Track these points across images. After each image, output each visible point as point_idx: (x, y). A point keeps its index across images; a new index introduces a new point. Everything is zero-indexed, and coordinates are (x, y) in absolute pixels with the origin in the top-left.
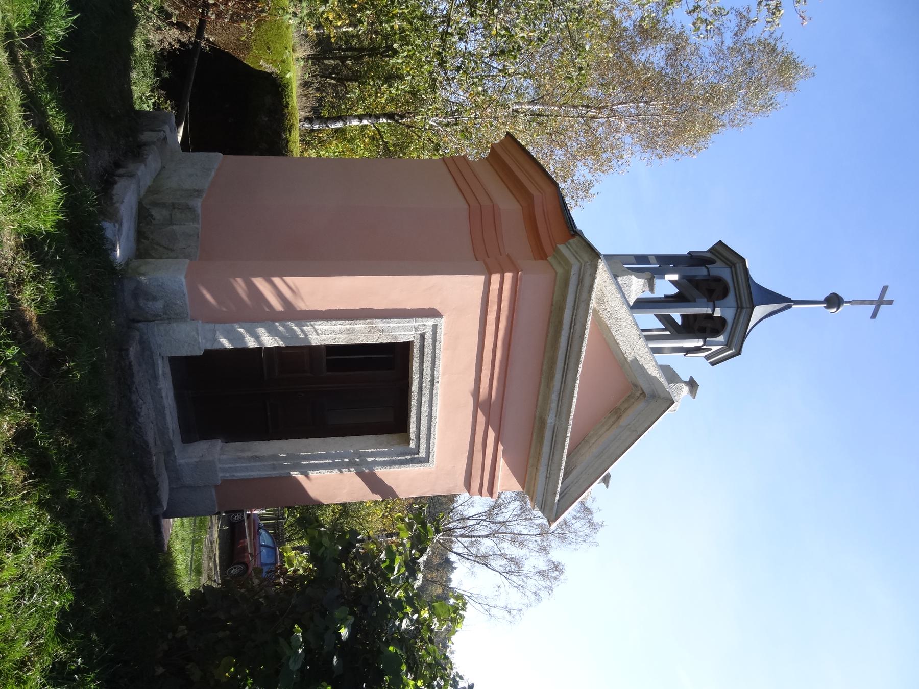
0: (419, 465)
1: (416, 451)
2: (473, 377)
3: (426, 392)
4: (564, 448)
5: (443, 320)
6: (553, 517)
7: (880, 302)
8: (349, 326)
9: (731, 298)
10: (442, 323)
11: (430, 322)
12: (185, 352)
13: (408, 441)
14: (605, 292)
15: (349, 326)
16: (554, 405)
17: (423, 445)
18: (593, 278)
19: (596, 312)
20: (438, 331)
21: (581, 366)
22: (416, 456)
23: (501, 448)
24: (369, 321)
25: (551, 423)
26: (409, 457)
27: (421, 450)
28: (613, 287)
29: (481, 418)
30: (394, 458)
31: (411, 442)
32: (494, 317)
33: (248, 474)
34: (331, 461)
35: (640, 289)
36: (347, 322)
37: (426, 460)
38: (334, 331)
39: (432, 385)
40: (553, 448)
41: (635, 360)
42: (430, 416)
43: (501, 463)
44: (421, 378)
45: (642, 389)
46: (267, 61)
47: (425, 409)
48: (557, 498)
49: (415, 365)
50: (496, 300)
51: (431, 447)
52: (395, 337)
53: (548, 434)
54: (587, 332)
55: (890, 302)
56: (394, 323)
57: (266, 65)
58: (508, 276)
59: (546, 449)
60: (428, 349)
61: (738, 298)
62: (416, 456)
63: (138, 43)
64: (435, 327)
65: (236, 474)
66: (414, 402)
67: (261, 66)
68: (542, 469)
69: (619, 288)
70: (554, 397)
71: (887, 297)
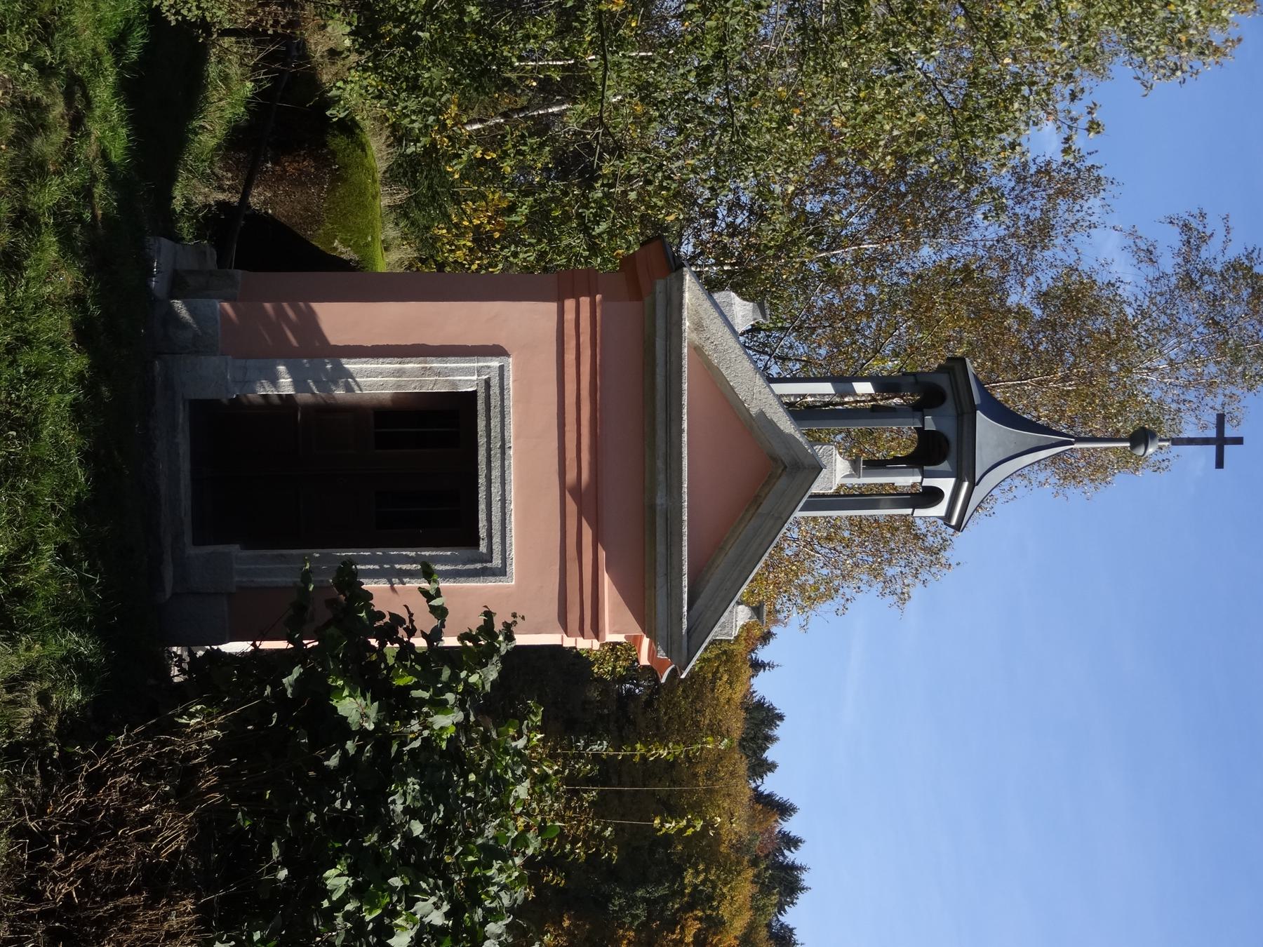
1: (488, 558)
2: (555, 444)
3: (496, 464)
5: (511, 360)
6: (684, 659)
7: (1221, 442)
8: (398, 366)
9: (949, 407)
10: (510, 362)
11: (495, 363)
12: (209, 394)
13: (476, 544)
14: (702, 314)
15: (398, 366)
16: (661, 477)
17: (497, 547)
19: (697, 349)
20: (506, 374)
21: (685, 411)
22: (489, 565)
23: (602, 555)
24: (421, 359)
25: (662, 505)
26: (479, 566)
27: (495, 556)
28: (707, 304)
29: (572, 507)
30: (460, 567)
31: (481, 542)
32: (574, 357)
33: (269, 580)
34: (377, 567)
35: (750, 316)
36: (396, 360)
37: (502, 572)
38: (381, 373)
39: (503, 453)
40: (669, 546)
41: (762, 414)
42: (503, 500)
43: (606, 581)
44: (489, 442)
45: (783, 463)
46: (343, 242)
47: (496, 489)
48: (685, 626)
49: (481, 424)
50: (573, 333)
51: (508, 549)
52: (453, 383)
53: (660, 522)
54: (685, 362)
55: (1238, 441)
57: (341, 248)
58: (585, 301)
59: (661, 549)
60: (495, 401)
61: (958, 404)
62: (489, 565)
63: (178, 204)
64: (501, 368)
65: (255, 579)
66: (482, 480)
67: (336, 249)
68: (660, 581)
69: (715, 305)
70: (660, 464)
71: (1229, 432)
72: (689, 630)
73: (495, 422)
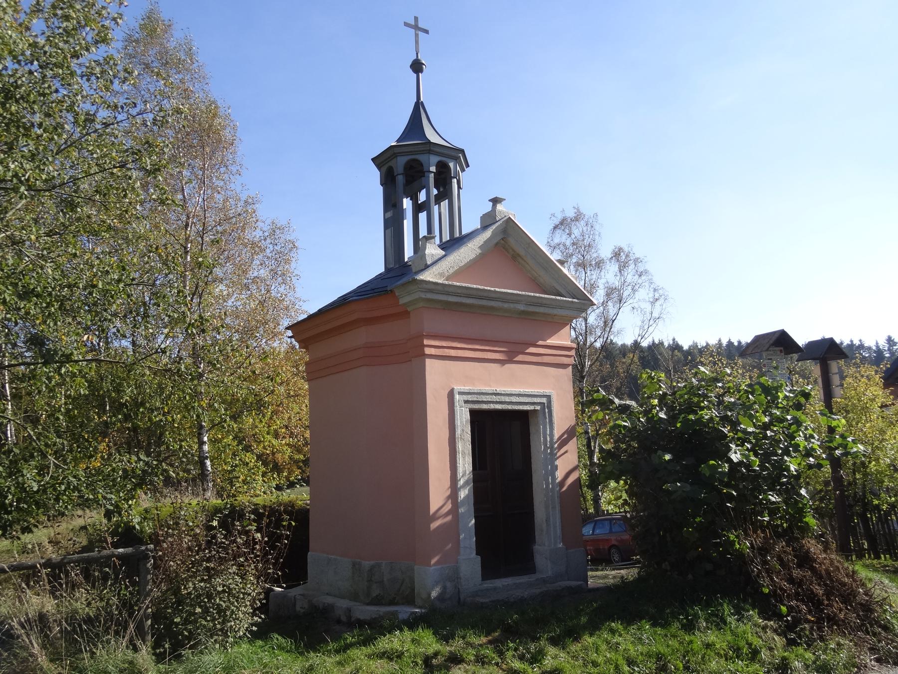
0: (552, 402)
1: (543, 405)
3: (503, 399)
4: (542, 297)
5: (455, 388)
6: (589, 303)
7: (416, 27)
9: (422, 158)
10: (458, 388)
11: (457, 397)
13: (535, 411)
16: (512, 306)
18: (429, 282)
20: (462, 391)
21: (486, 288)
23: (540, 343)
26: (547, 410)
29: (520, 358)
30: (547, 420)
36: (457, 456)
37: (549, 397)
40: (541, 305)
41: (480, 247)
42: (519, 395)
43: (550, 342)
47: (514, 399)
48: (576, 300)
49: (485, 407)
52: (466, 422)
53: (531, 309)
54: (464, 285)
55: (416, 19)
56: (458, 423)
58: (426, 342)
59: (541, 310)
61: (422, 152)
64: (460, 393)
66: (510, 407)
68: (555, 312)
70: (506, 305)
72: (578, 299)
73: (484, 398)
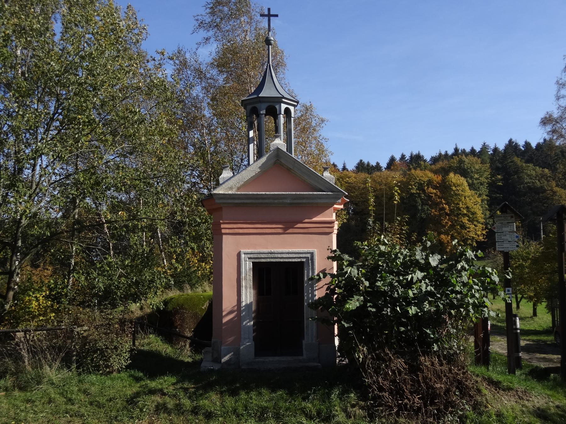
0: (314, 257)
2: (270, 236)
3: (276, 256)
6: (341, 193)
7: (269, 16)
9: (258, 106)
11: (243, 256)
12: (252, 350)
13: (302, 263)
16: (281, 201)
18: (219, 194)
19: (239, 189)
21: (259, 193)
22: (310, 258)
23: (306, 220)
26: (310, 261)
27: (307, 256)
28: (224, 185)
29: (290, 231)
30: (310, 268)
35: (228, 171)
41: (260, 168)
42: (288, 253)
43: (315, 219)
44: (269, 258)
46: (203, 305)
47: (284, 256)
48: (330, 193)
52: (250, 269)
54: (243, 193)
55: (269, 9)
56: (243, 270)
57: (205, 306)
58: (222, 226)
59: (304, 201)
60: (255, 256)
62: (310, 258)
63: (190, 360)
64: (245, 254)
66: (282, 260)
67: (205, 308)
68: (316, 201)
70: (276, 201)
72: (332, 192)
73: (262, 256)
